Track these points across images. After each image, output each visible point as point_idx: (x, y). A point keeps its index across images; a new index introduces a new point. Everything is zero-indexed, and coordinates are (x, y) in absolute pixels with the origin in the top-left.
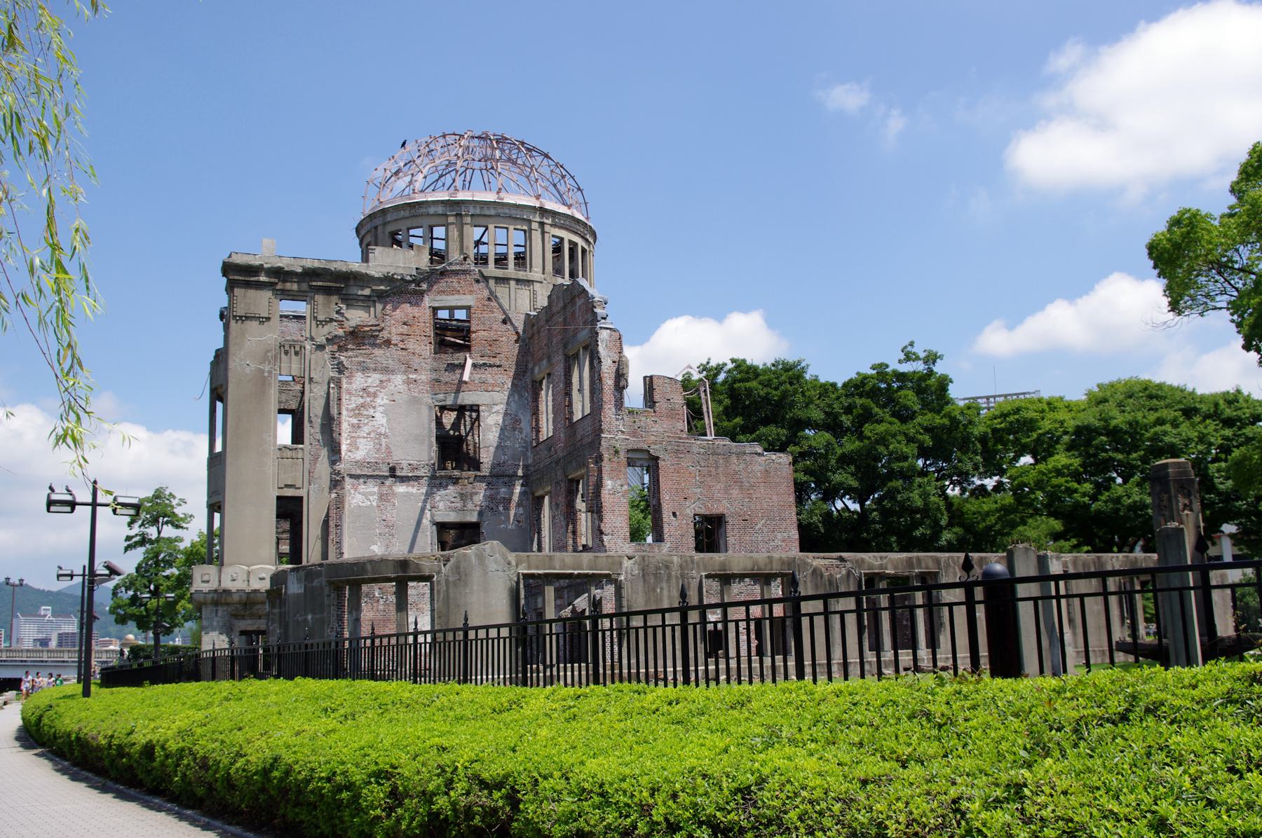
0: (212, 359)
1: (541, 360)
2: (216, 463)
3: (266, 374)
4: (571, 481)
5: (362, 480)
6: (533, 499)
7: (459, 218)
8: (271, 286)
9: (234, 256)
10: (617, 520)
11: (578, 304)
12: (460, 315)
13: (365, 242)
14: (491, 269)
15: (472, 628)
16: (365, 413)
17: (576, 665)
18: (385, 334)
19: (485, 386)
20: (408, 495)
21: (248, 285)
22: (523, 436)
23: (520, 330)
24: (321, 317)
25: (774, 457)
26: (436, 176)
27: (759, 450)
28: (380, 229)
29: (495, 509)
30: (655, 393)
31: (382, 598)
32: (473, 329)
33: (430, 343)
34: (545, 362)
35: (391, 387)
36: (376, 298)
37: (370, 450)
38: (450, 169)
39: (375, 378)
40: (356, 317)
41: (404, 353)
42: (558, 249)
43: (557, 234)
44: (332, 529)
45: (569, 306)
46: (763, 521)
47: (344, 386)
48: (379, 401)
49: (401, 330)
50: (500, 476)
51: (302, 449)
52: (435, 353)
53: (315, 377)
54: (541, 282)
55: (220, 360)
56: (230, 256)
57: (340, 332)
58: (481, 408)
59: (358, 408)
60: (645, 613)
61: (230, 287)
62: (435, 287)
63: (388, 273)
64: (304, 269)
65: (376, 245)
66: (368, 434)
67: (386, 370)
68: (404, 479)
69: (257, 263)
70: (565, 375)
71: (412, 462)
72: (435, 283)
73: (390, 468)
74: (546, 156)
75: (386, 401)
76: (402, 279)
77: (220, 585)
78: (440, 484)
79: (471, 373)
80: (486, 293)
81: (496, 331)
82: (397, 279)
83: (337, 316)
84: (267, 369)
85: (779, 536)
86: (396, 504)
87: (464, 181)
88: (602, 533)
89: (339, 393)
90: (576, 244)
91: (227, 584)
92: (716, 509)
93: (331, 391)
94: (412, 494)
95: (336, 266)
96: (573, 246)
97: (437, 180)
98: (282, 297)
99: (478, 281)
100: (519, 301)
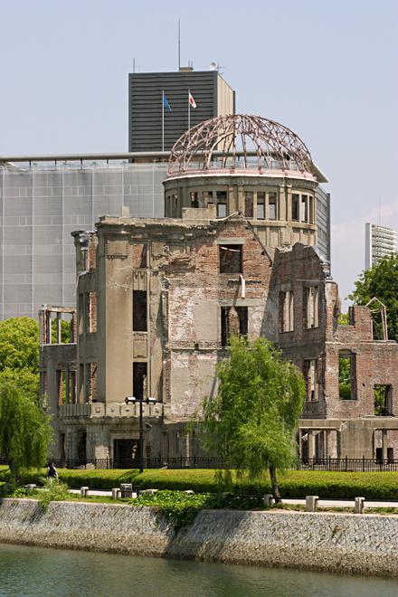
10: (333, 390)
18: (192, 263)
23: (272, 259)
28: (184, 190)
40: (176, 254)
44: (164, 382)
47: (169, 295)
48: (188, 304)
57: (167, 263)
67: (192, 285)
68: (203, 352)
80: (252, 236)
84: (126, 287)
88: (324, 395)
90: (306, 196)
91: (109, 413)
94: (207, 361)
99: (247, 228)
100: (272, 240)
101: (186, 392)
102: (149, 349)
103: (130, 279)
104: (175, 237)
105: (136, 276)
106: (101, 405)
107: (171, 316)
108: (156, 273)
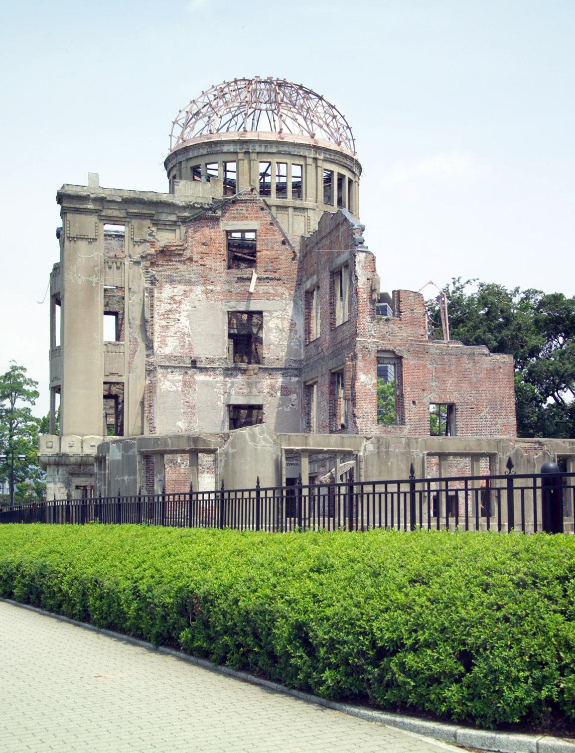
0: (51, 271)
1: (312, 275)
2: (55, 353)
4: (333, 374)
5: (169, 370)
6: (305, 388)
7: (247, 156)
8: (96, 212)
9: (66, 188)
10: (367, 408)
11: (341, 230)
12: (250, 236)
13: (172, 174)
14: (273, 199)
15: (263, 489)
16: (173, 316)
17: (293, 519)
18: (187, 254)
19: (268, 296)
20: (207, 384)
21: (78, 211)
22: (298, 336)
23: (297, 249)
25: (498, 357)
26: (230, 116)
27: (486, 351)
28: (183, 165)
29: (274, 394)
30: (401, 305)
31: (183, 464)
32: (258, 249)
33: (224, 260)
34: (315, 277)
35: (192, 295)
36: (180, 223)
37: (176, 346)
38: (242, 110)
39: (180, 288)
40: (165, 238)
41: (203, 268)
42: (328, 180)
43: (328, 168)
45: (334, 232)
46: (487, 409)
47: (156, 295)
48: (183, 307)
50: (279, 368)
51: (123, 345)
52: (229, 268)
53: (133, 287)
54: (314, 210)
55: (57, 271)
56: (63, 188)
57: (152, 251)
58: (264, 314)
59: (167, 312)
60: (374, 484)
61: (63, 214)
62: (228, 214)
63: (190, 202)
64: (122, 199)
65: (181, 178)
66: (175, 333)
67: (188, 282)
68: (202, 370)
69: (85, 194)
70: (330, 288)
71: (209, 356)
72: (228, 210)
73: (192, 361)
74: (321, 98)
75: (188, 307)
76: (201, 207)
77: (60, 450)
78: (232, 374)
79: (256, 285)
80: (269, 219)
81: (277, 250)
82: (197, 208)
83: (150, 238)
84: (95, 280)
85: (500, 422)
86: (197, 389)
87: (253, 119)
88: (355, 416)
89: (152, 301)
92: (449, 399)
93: (146, 299)
95: (148, 196)
96: (341, 178)
97: (231, 120)
98: (105, 222)
99: (262, 209)
100: (296, 226)
101: (179, 424)
102: (127, 365)
103: (101, 271)
104: (164, 217)
105: (110, 268)
106: (55, 438)
107: (158, 322)
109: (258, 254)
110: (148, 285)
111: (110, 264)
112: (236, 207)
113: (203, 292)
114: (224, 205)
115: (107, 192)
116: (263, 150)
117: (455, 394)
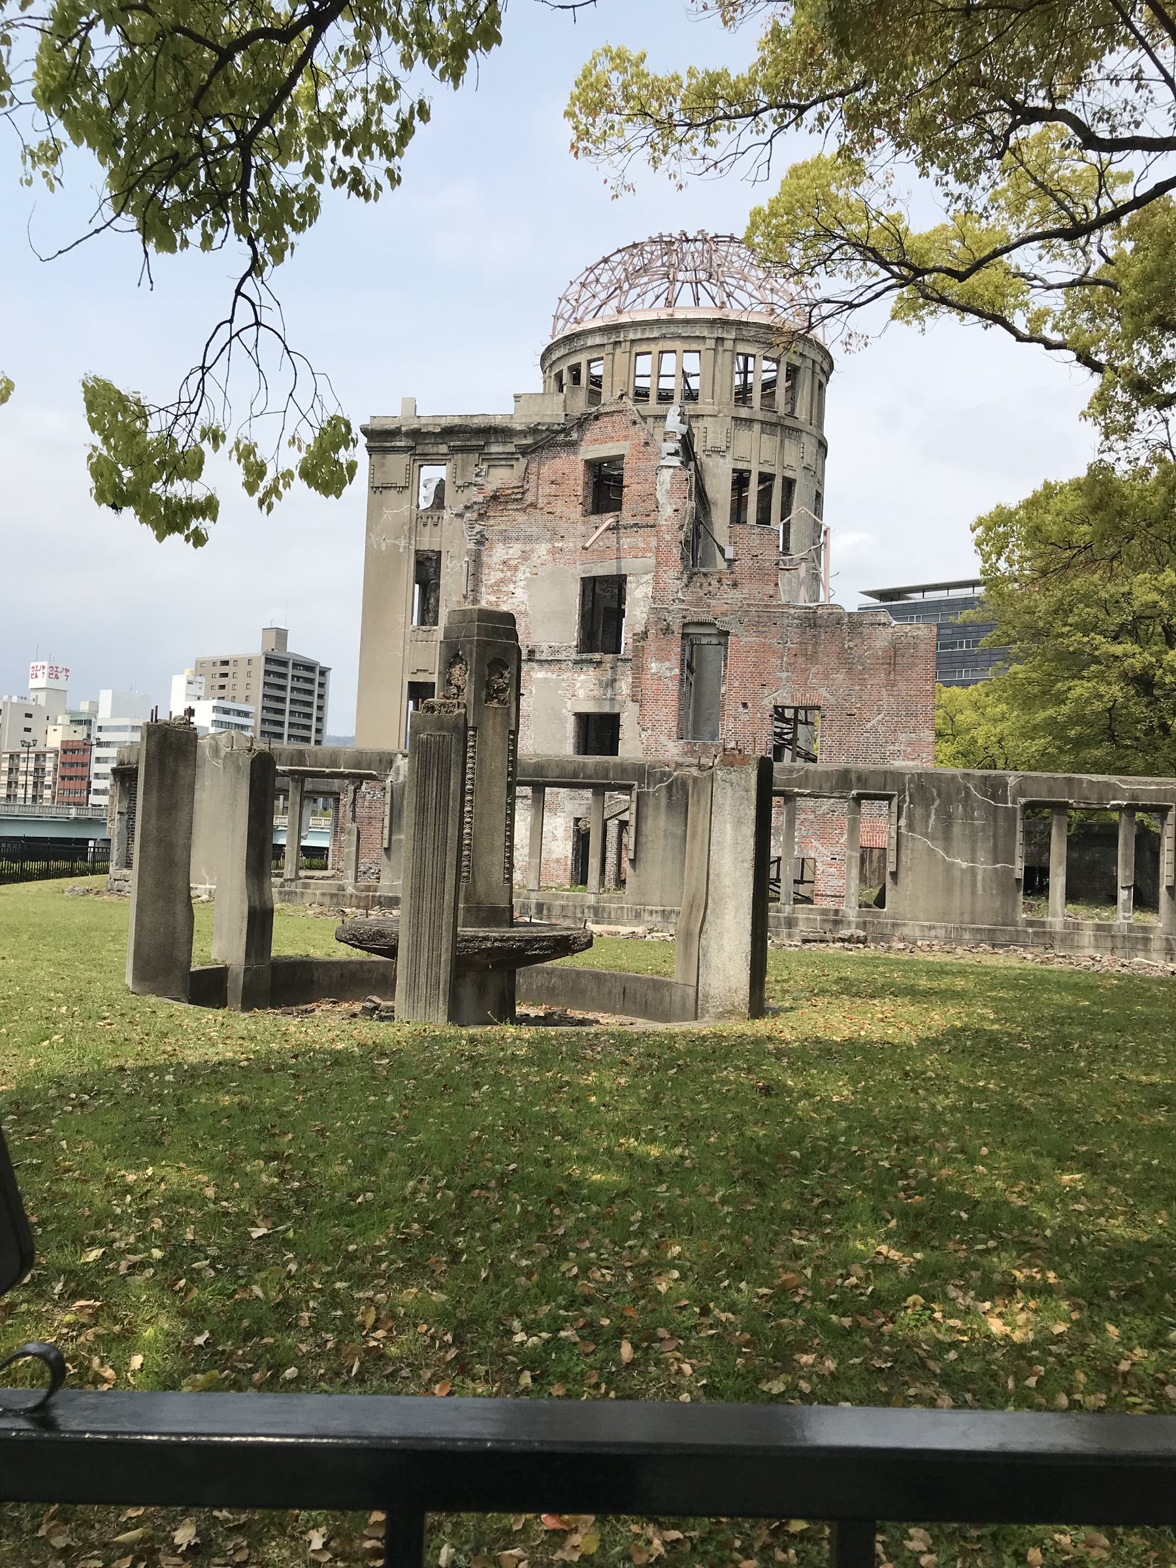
3: (401, 550)
14: (652, 406)
16: (505, 589)
21: (386, 451)
24: (459, 482)
39: (516, 549)
40: (500, 478)
41: (551, 517)
48: (520, 575)
49: (547, 491)
57: (480, 499)
59: (498, 583)
67: (529, 539)
69: (393, 427)
80: (643, 436)
82: (542, 431)
99: (635, 423)
108: (460, 516)
109: (625, 490)
110: (472, 546)
111: (424, 520)
112: (599, 423)
113: (549, 552)
114: (582, 423)
115: (423, 421)
116: (639, 336)
117: (823, 692)
